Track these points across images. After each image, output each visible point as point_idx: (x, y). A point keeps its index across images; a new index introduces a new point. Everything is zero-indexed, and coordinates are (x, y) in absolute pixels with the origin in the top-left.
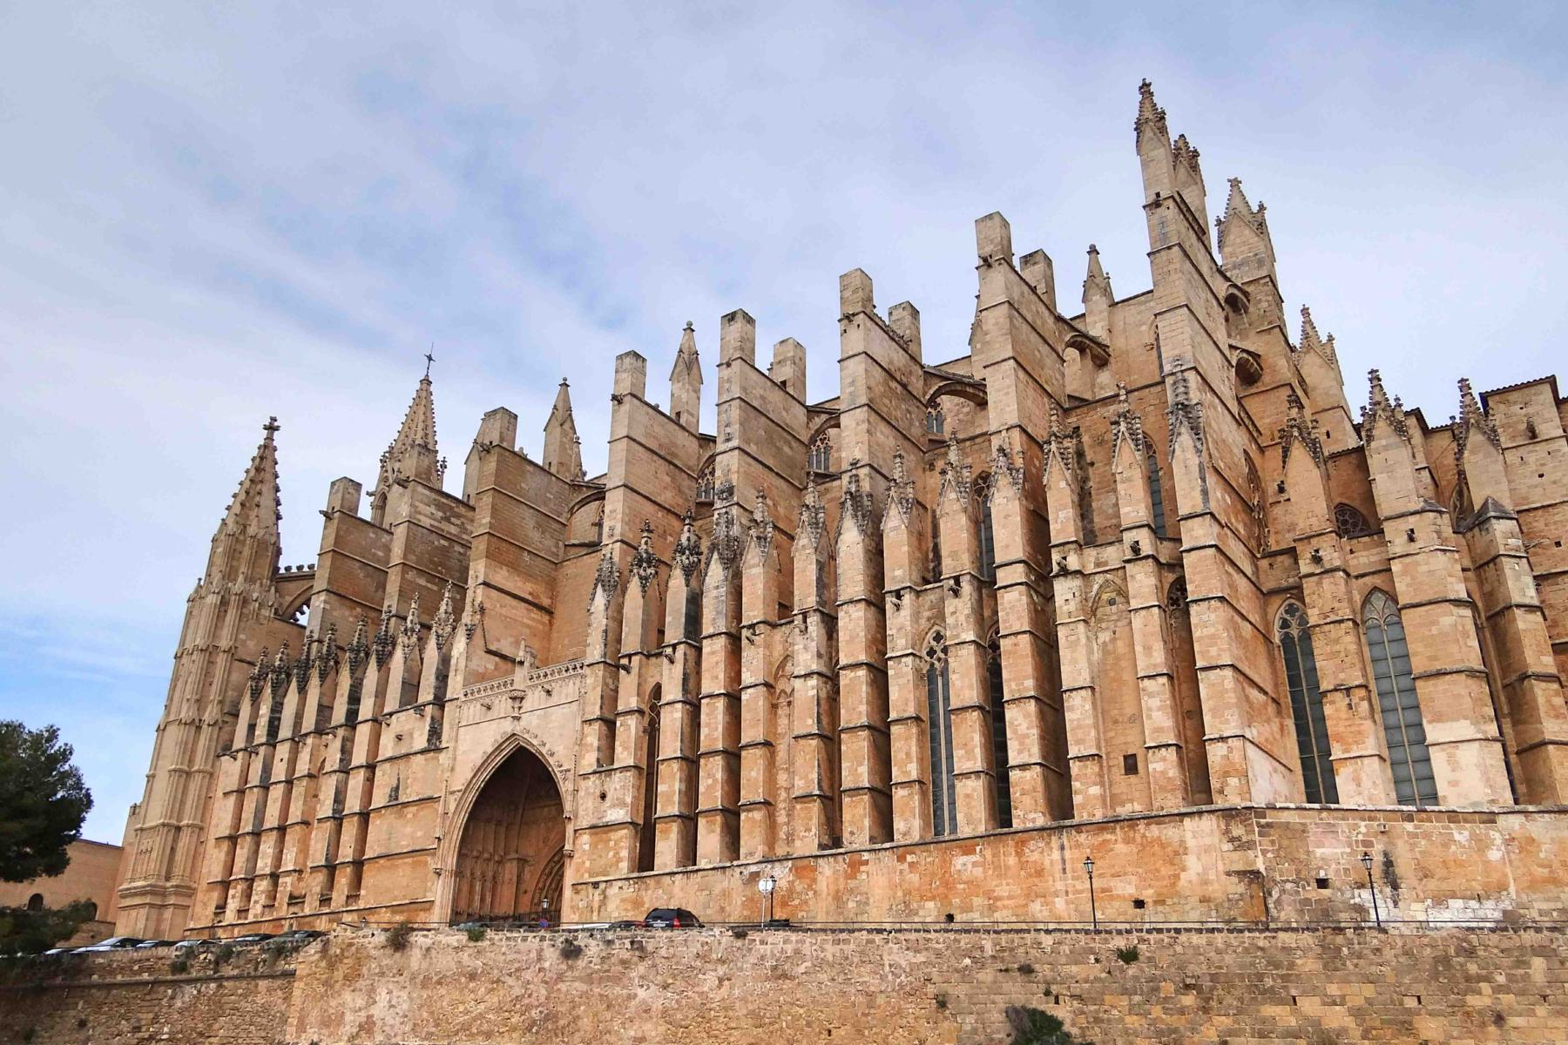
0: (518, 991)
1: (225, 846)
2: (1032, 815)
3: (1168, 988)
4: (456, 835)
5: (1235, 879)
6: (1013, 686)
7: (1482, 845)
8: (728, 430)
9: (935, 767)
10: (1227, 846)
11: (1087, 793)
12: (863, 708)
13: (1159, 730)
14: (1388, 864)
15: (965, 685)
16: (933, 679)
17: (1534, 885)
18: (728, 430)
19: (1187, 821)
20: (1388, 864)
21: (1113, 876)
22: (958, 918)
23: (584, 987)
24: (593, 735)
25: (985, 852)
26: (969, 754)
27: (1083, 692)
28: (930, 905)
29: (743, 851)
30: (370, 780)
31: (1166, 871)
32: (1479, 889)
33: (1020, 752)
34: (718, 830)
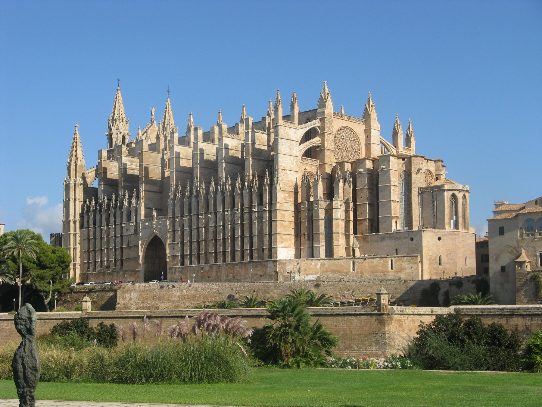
0: (155, 293)
1: (87, 253)
5: (274, 272)
7: (316, 265)
10: (273, 266)
11: (256, 255)
14: (299, 269)
15: (238, 233)
17: (323, 272)
20: (299, 269)
21: (258, 271)
22: (235, 277)
23: (165, 292)
28: (231, 275)
30: (122, 239)
31: (265, 270)
32: (314, 272)
34: (196, 258)
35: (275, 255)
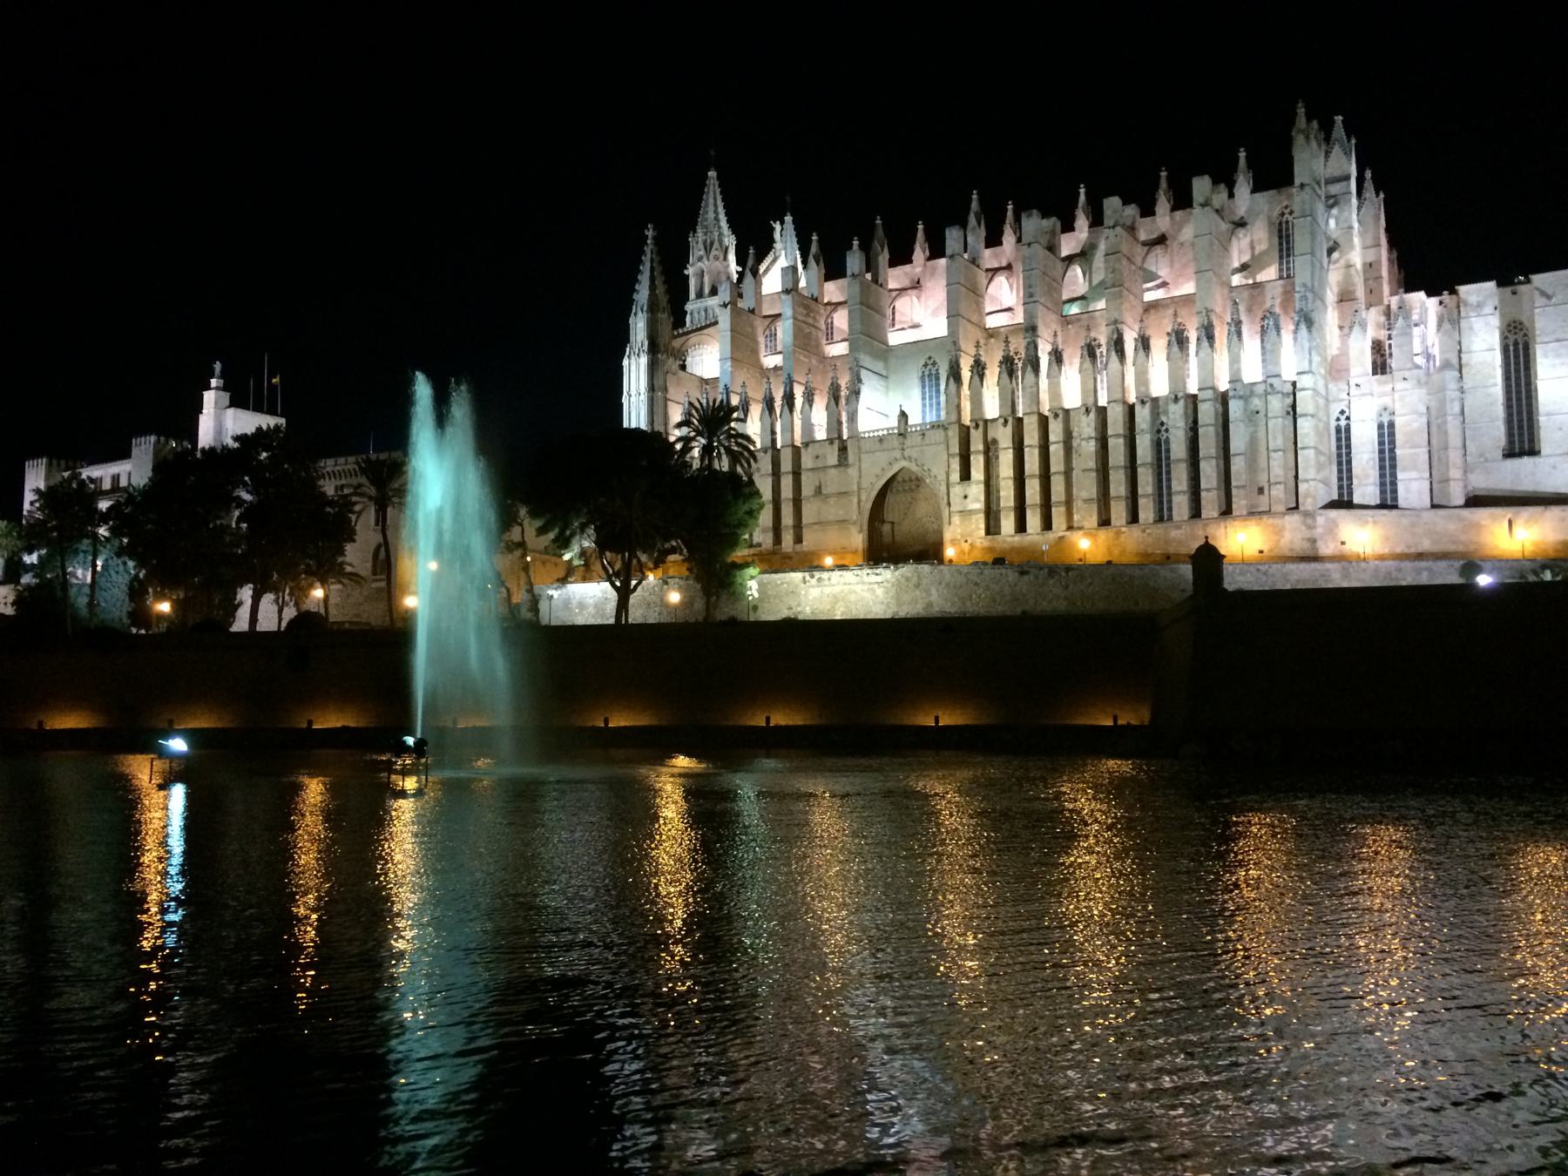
4: (866, 515)
8: (1031, 290)
9: (1160, 488)
10: (1304, 528)
11: (1239, 504)
12: (1122, 458)
13: (1277, 476)
15: (1179, 449)
16: (1160, 447)
18: (1031, 290)
19: (1287, 517)
24: (956, 465)
25: (1186, 529)
26: (1180, 484)
27: (1242, 457)
29: (1054, 526)
35: (1309, 500)
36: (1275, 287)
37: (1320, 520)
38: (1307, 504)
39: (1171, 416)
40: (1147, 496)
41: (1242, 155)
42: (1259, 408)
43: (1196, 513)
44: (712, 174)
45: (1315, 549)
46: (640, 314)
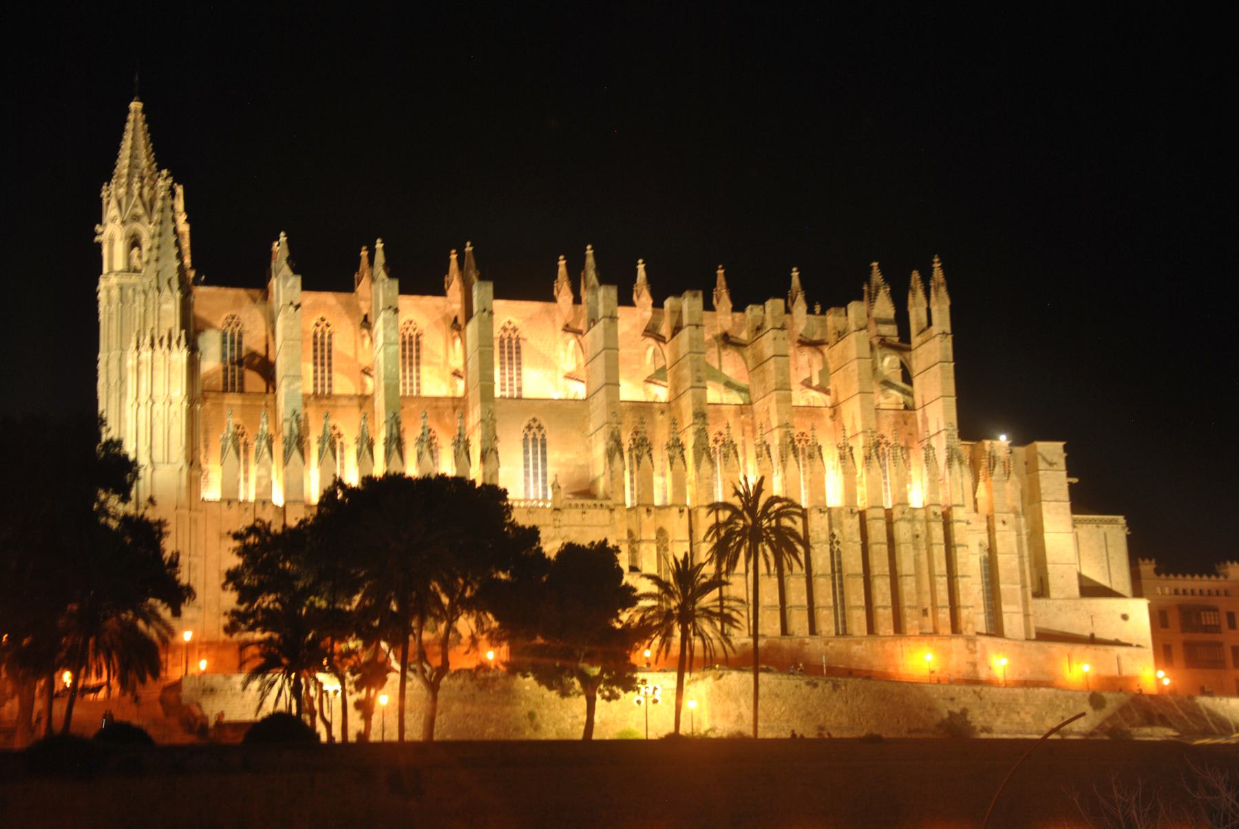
2: (888, 631)
3: (989, 707)
6: (880, 569)
8: (699, 374)
10: (967, 652)
11: (912, 622)
18: (699, 374)
19: (953, 640)
33: (883, 600)
35: (970, 626)
36: (887, 416)
37: (978, 644)
38: (969, 630)
39: (846, 530)
40: (827, 608)
41: (795, 275)
42: (919, 532)
43: (871, 629)
44: (135, 105)
45: (975, 672)
46: (166, 292)
